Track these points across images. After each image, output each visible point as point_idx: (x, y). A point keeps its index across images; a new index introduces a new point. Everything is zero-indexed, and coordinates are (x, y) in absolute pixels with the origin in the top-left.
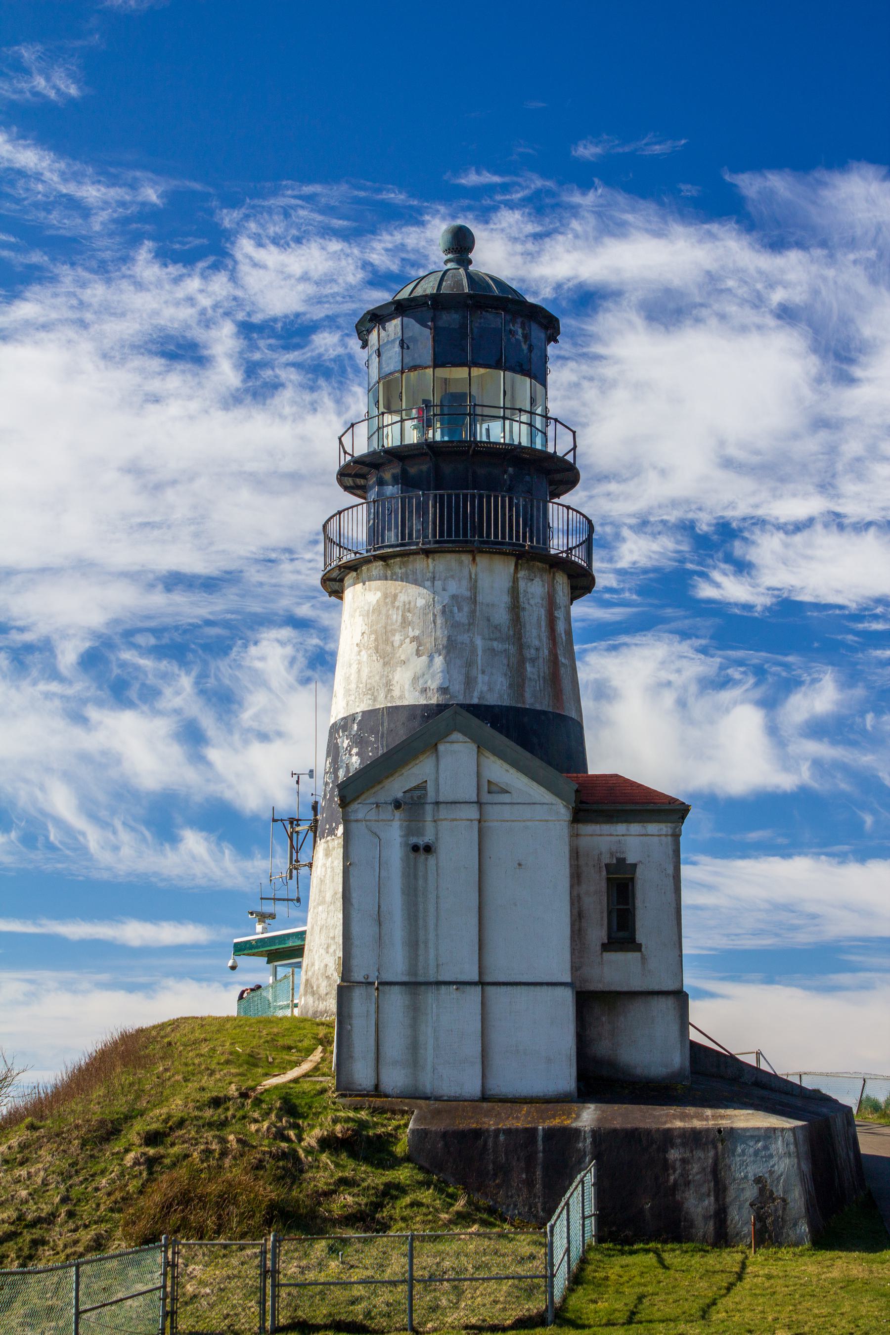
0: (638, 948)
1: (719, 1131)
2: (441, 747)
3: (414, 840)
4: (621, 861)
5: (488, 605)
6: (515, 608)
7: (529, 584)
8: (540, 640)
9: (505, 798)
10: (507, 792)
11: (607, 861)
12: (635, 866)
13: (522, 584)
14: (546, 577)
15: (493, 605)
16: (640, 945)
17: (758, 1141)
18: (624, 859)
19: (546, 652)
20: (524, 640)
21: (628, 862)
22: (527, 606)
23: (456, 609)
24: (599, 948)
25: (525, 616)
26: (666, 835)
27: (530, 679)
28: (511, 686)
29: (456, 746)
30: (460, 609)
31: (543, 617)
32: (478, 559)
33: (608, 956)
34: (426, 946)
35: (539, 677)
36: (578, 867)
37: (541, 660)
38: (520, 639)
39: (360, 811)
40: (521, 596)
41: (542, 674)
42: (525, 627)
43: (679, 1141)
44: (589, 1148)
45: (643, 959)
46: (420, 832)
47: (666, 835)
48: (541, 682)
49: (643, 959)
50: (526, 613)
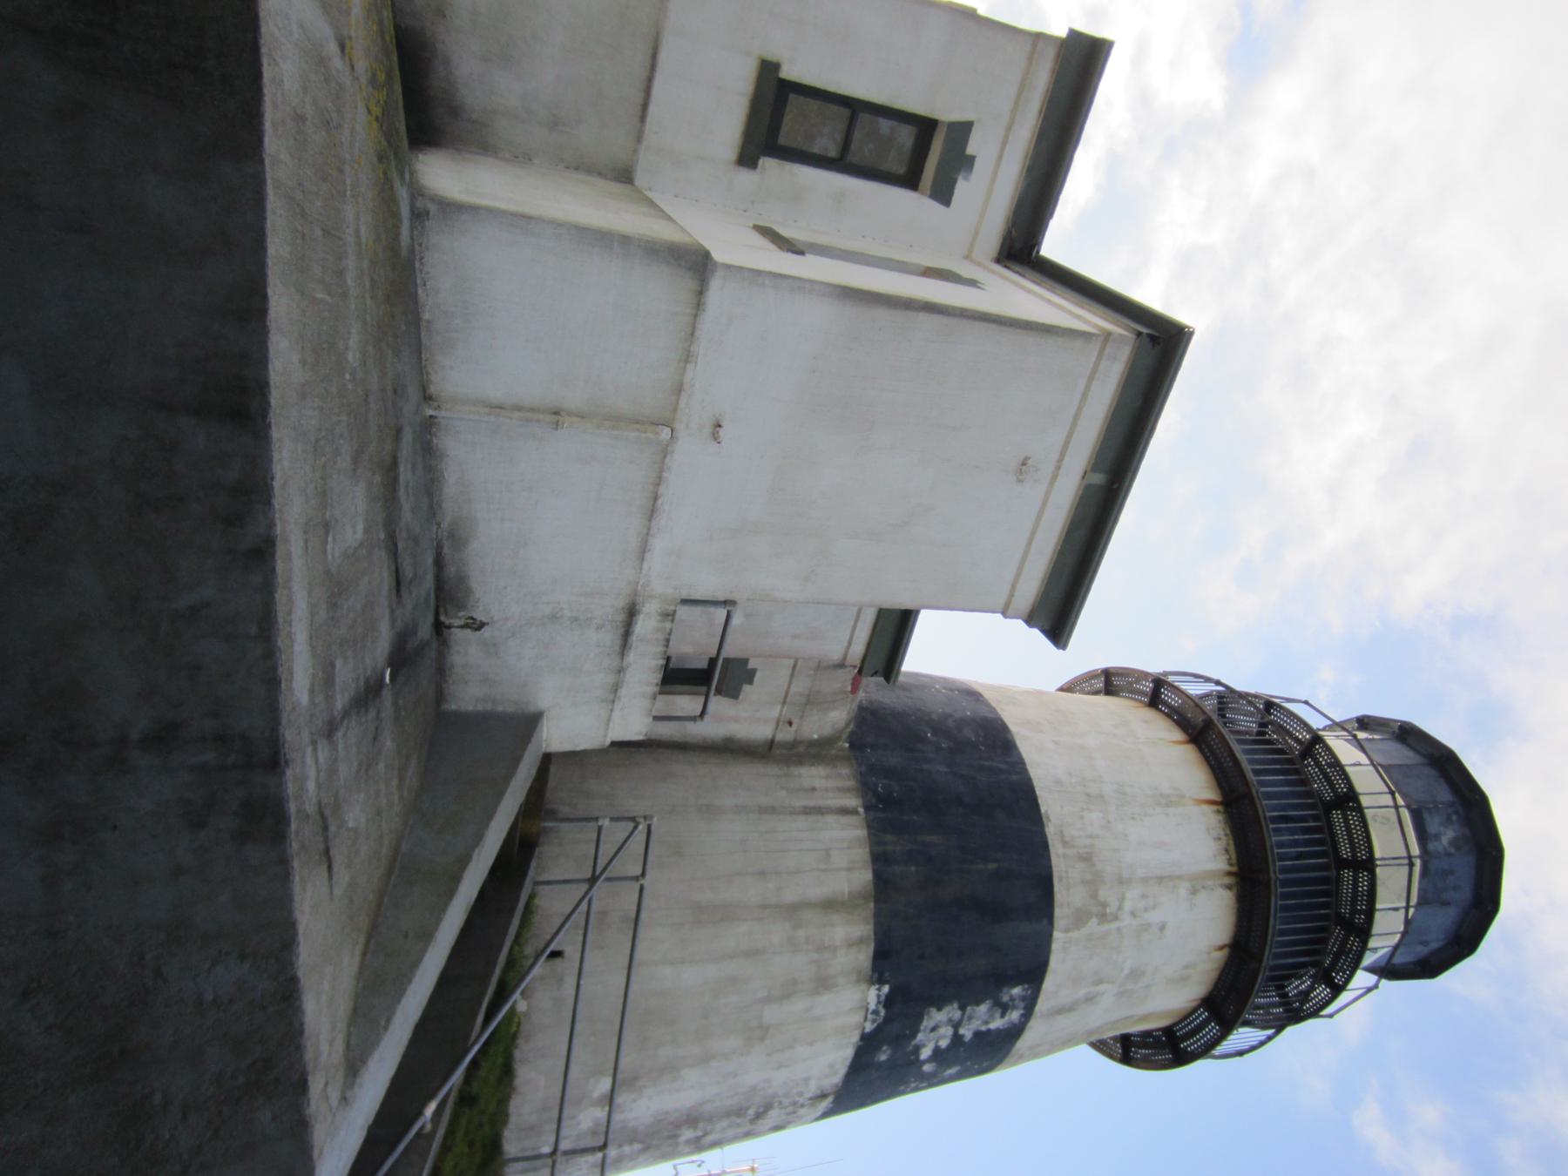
35: (1091, 837)
48: (1087, 842)
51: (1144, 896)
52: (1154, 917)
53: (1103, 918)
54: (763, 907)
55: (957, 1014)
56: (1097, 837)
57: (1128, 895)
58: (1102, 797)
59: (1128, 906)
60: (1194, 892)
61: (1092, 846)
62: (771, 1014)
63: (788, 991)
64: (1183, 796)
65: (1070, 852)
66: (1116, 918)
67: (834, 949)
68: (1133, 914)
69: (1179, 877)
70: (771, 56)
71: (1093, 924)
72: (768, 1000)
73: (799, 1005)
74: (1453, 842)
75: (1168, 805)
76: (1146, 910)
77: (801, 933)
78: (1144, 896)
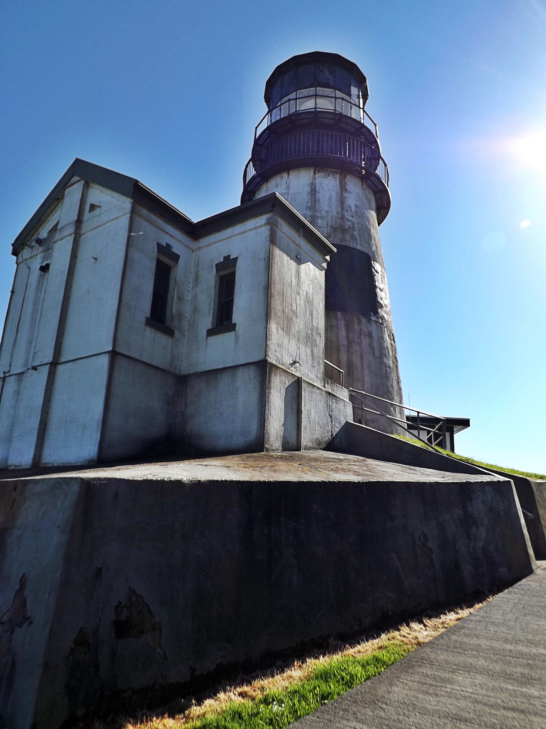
5: (295, 194)
7: (324, 179)
8: (330, 206)
11: (217, 262)
12: (236, 259)
15: (299, 193)
19: (334, 213)
20: (317, 207)
21: (231, 258)
22: (321, 191)
24: (205, 333)
25: (319, 196)
31: (334, 196)
32: (290, 173)
33: (212, 339)
35: (327, 225)
36: (197, 272)
37: (330, 218)
38: (315, 207)
40: (317, 186)
41: (329, 224)
42: (319, 201)
45: (237, 337)
48: (329, 228)
49: (237, 337)
50: (321, 195)
51: (347, 211)
52: (353, 208)
53: (354, 229)
54: (348, 352)
56: (327, 223)
57: (347, 217)
58: (311, 217)
59: (350, 218)
60: (346, 190)
61: (331, 226)
64: (312, 183)
65: (332, 236)
66: (353, 224)
67: (361, 329)
68: (353, 217)
69: (342, 194)
70: (143, 320)
71: (356, 233)
72: (374, 354)
74: (331, 73)
75: (315, 191)
76: (351, 211)
77: (356, 340)
78: (347, 211)
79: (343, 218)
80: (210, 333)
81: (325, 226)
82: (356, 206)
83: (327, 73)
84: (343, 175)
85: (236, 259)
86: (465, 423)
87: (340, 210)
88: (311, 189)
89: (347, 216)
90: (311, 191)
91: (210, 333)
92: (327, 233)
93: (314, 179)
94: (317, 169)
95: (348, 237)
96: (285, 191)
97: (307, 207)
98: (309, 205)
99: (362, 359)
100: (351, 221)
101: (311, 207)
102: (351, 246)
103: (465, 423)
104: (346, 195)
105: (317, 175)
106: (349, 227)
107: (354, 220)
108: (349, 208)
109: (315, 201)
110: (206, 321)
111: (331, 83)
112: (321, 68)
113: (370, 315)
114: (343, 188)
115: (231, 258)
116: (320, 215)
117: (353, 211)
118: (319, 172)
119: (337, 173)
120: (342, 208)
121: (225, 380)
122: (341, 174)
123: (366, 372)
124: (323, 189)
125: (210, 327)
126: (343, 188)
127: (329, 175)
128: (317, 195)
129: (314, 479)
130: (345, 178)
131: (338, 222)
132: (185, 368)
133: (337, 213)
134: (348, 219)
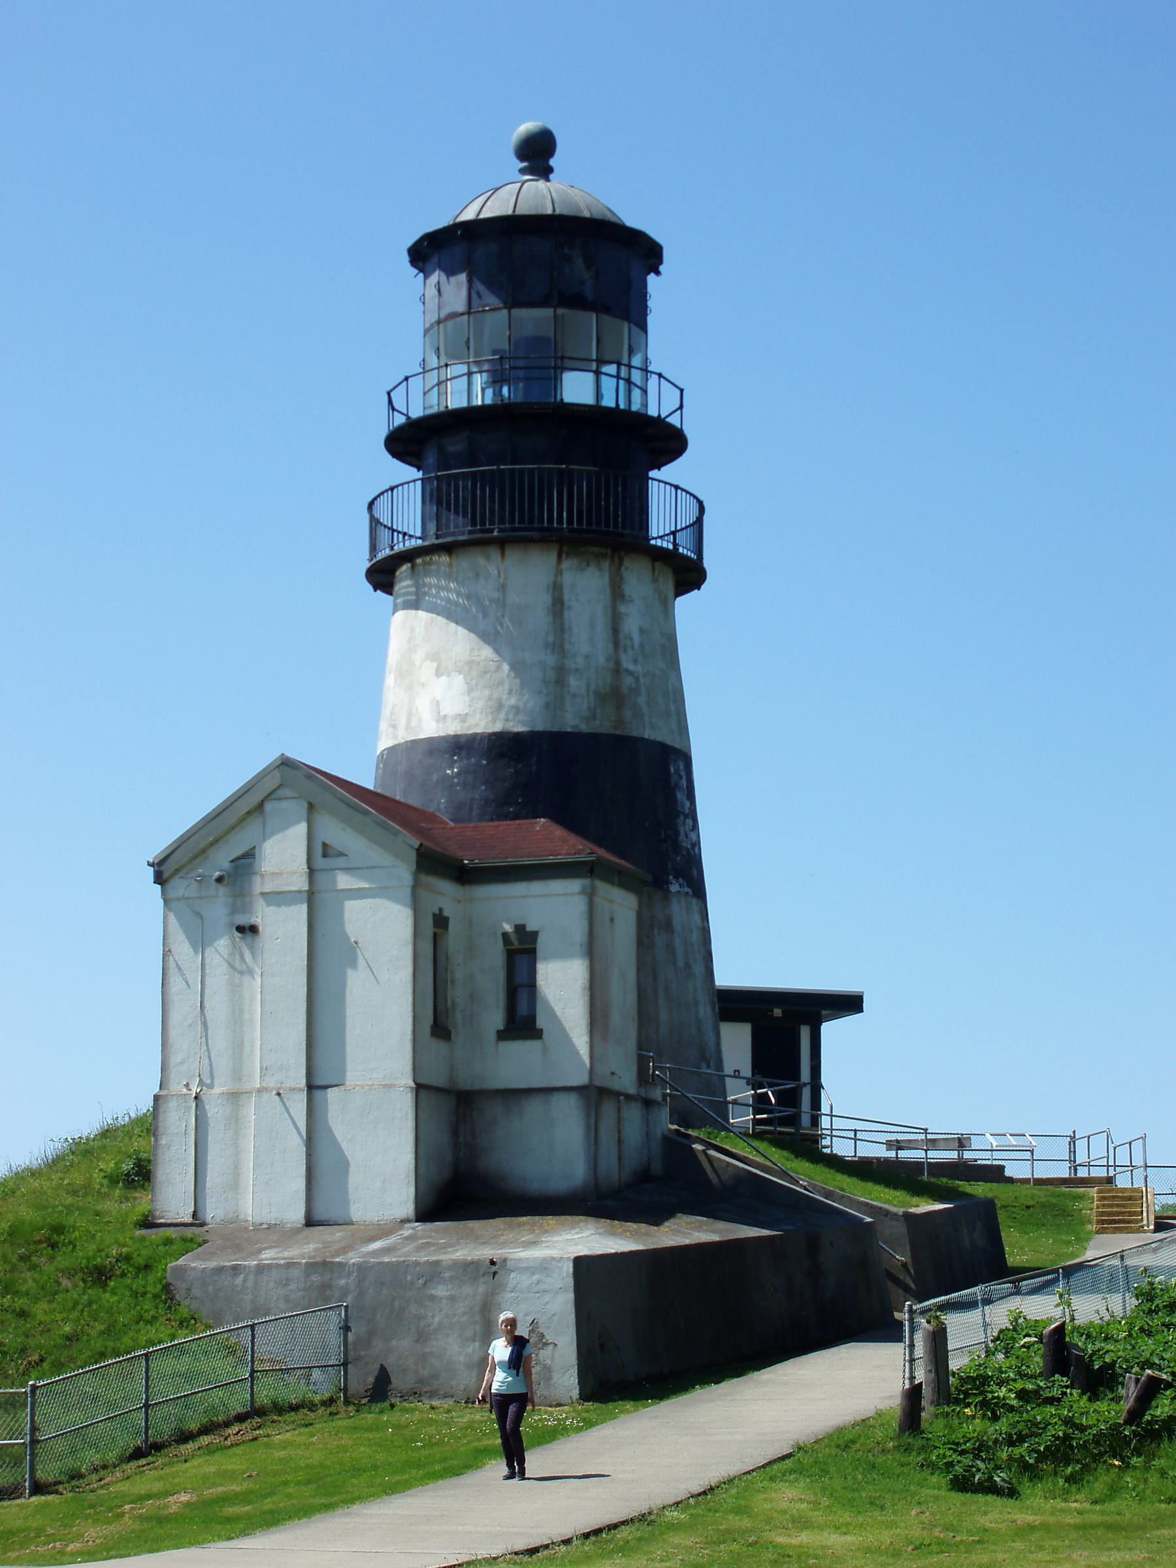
0: (537, 1034)
1: (493, 1263)
2: (268, 806)
3: (241, 920)
4: (520, 929)
6: (558, 606)
9: (341, 862)
10: (341, 854)
13: (568, 578)
14: (606, 564)
16: (541, 1030)
17: (533, 1273)
18: (524, 926)
19: (601, 659)
20: (567, 646)
23: (481, 616)
24: (493, 1036)
25: (570, 616)
26: (572, 894)
27: (574, 696)
28: (547, 706)
29: (284, 804)
30: (485, 616)
32: (507, 552)
34: (252, 1046)
35: (588, 690)
38: (562, 646)
39: (179, 887)
40: (566, 591)
41: (593, 687)
42: (570, 629)
43: (447, 1275)
44: (352, 1287)
45: (545, 1050)
46: (246, 908)
47: (572, 894)
48: (592, 698)
55: (682, 817)
56: (588, 685)
59: (631, 667)
60: (622, 596)
61: (595, 692)
62: (680, 964)
63: (670, 949)
64: (555, 583)
65: (598, 716)
66: (637, 679)
68: (635, 661)
72: (675, 964)
73: (678, 942)
75: (562, 603)
76: (633, 648)
78: (625, 651)
79: (617, 670)
80: (503, 1036)
81: (584, 692)
82: (642, 631)
83: (579, 263)
84: (616, 561)
85: (534, 935)
86: (851, 1004)
87: (611, 650)
88: (554, 598)
89: (627, 664)
90: (554, 605)
91: (503, 1036)
92: (589, 709)
93: (559, 573)
94: (565, 549)
95: (628, 714)
96: (496, 595)
97: (546, 645)
98: (551, 639)
99: (655, 978)
100: (630, 673)
101: (554, 643)
102: (635, 734)
103: (851, 1004)
104: (622, 609)
105: (566, 564)
106: (630, 689)
107: (639, 669)
108: (628, 642)
109: (562, 630)
110: (496, 1019)
111: (589, 292)
112: (566, 250)
113: (668, 883)
114: (617, 593)
115: (528, 929)
116: (573, 666)
117: (636, 646)
118: (568, 555)
119: (604, 556)
120: (616, 645)
121: (533, 1107)
122: (612, 558)
123: (662, 1002)
124: (577, 600)
125: (501, 1027)
126: (617, 593)
127: (588, 565)
128: (566, 615)
129: (687, 1242)
130: (620, 564)
131: (609, 682)
132: (465, 1082)
133: (607, 659)
134: (627, 671)
